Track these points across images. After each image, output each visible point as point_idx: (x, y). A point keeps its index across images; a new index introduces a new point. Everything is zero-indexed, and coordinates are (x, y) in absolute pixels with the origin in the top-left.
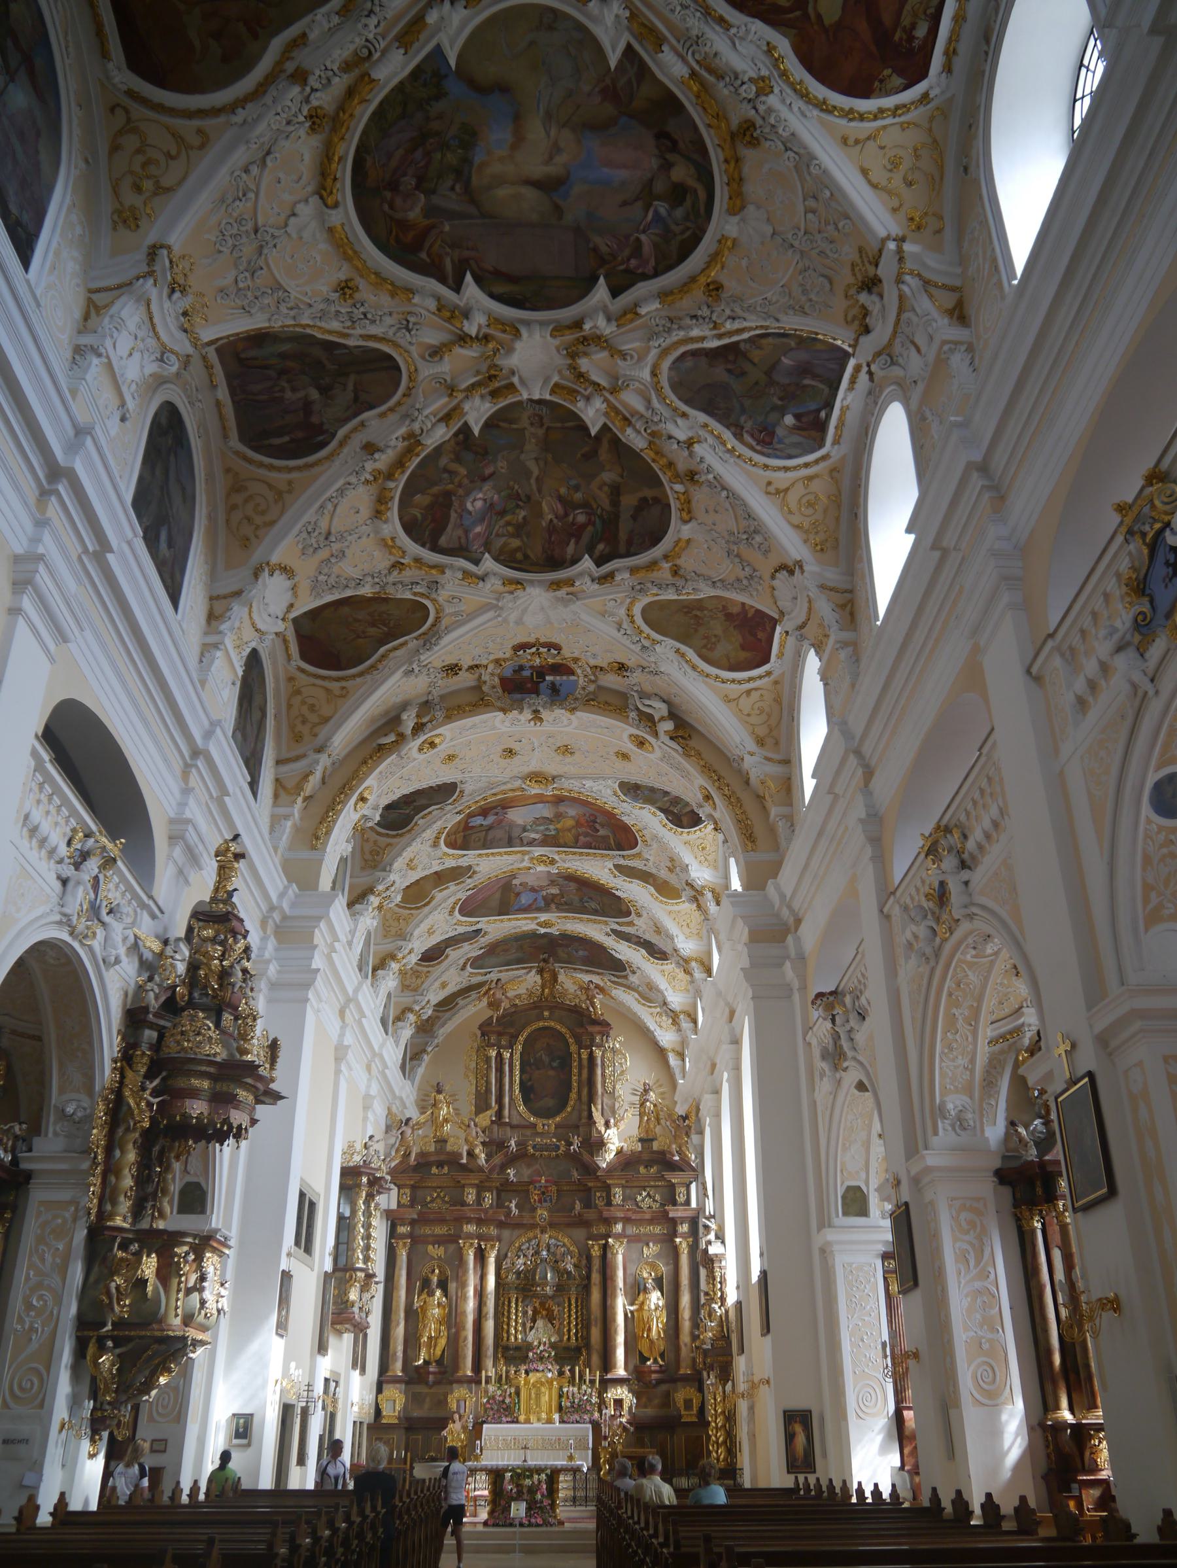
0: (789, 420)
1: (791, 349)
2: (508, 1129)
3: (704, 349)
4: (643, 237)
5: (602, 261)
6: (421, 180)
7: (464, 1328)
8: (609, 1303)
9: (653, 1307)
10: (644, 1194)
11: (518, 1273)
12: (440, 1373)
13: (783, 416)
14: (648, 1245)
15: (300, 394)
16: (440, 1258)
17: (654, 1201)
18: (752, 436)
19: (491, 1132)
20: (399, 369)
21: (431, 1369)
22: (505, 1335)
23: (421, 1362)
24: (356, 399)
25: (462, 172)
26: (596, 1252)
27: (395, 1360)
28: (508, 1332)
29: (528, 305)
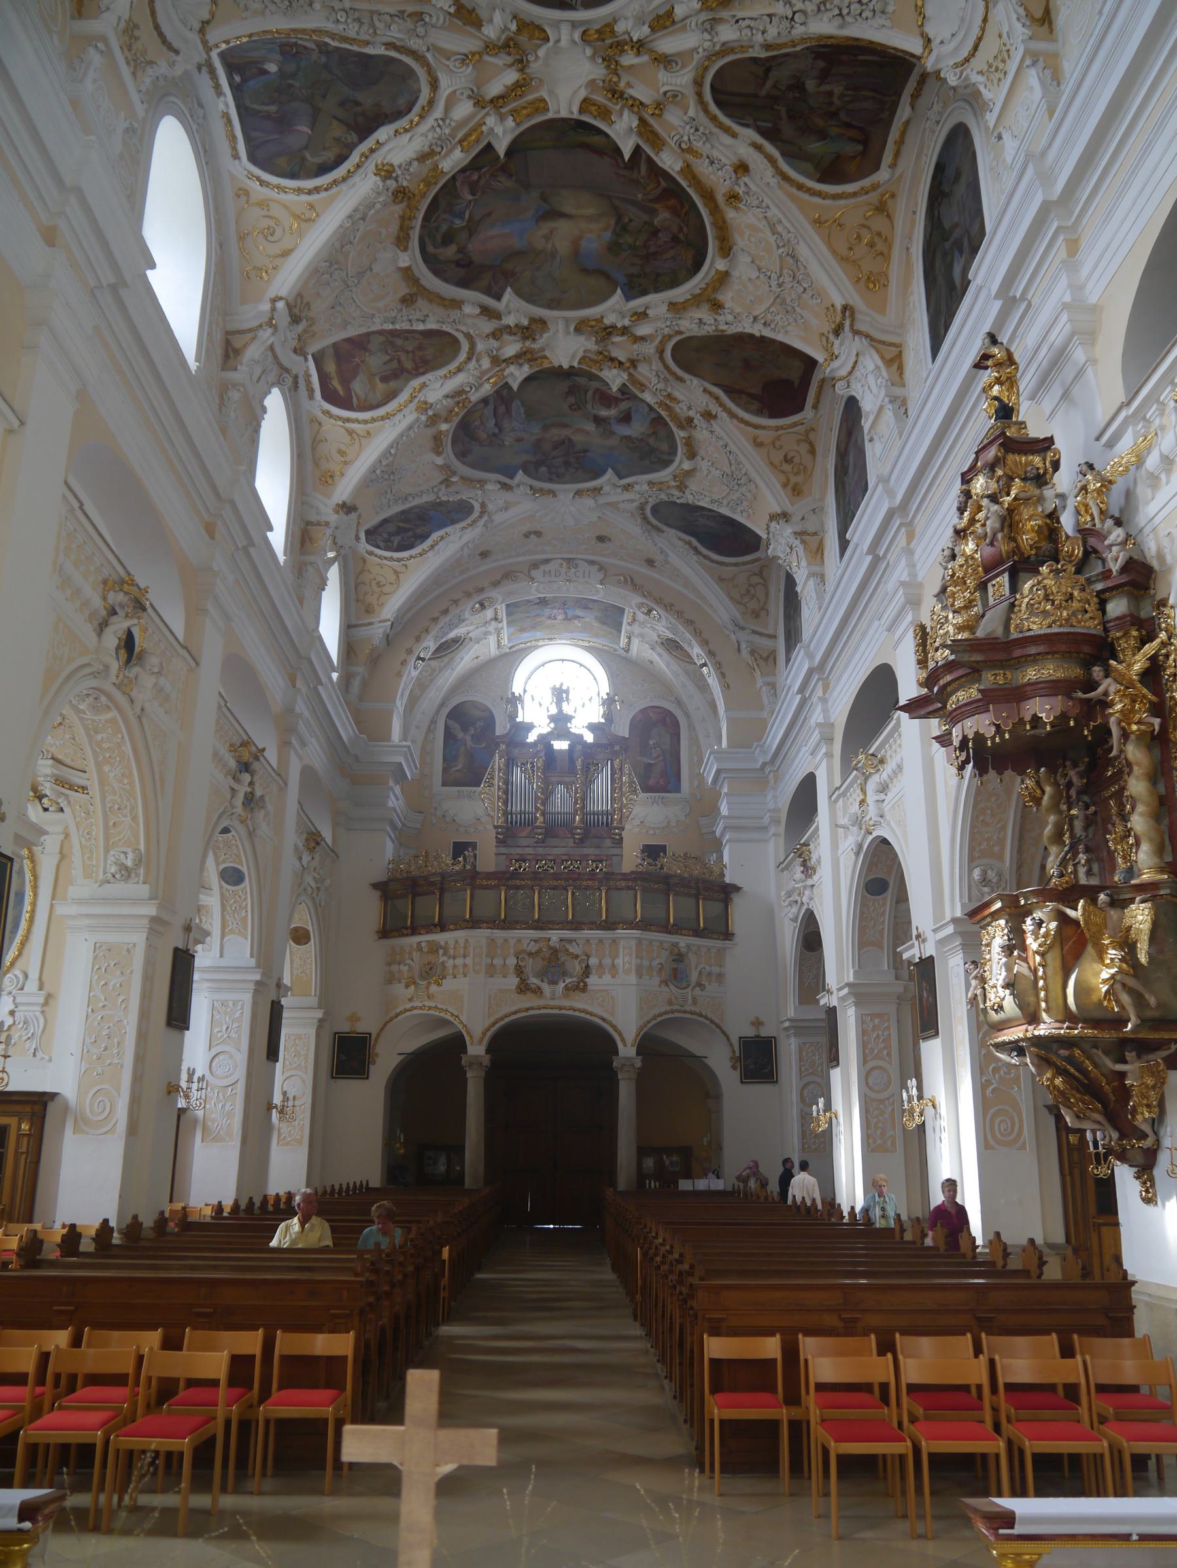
0: (272, 68)
1: (306, 147)
3: (391, 122)
4: (470, 197)
5: (504, 169)
6: (655, 233)
13: (280, 70)
15: (826, 88)
18: (305, 48)
20: (713, 88)
24: (768, 70)
25: (622, 228)
29: (572, 123)
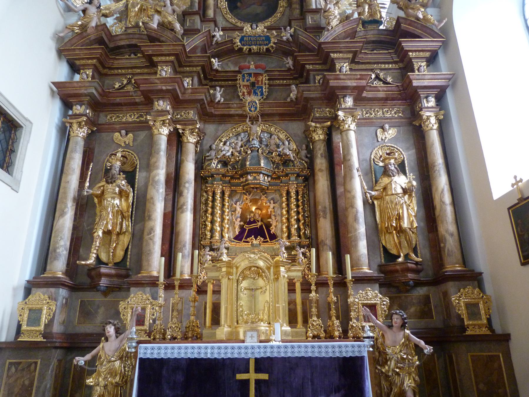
2: (212, 25)
7: (150, 218)
8: (340, 190)
9: (400, 191)
10: (373, 76)
11: (225, 163)
12: (118, 276)
14: (382, 128)
16: (127, 146)
17: (385, 83)
19: (193, 22)
21: (103, 270)
22: (209, 234)
23: (91, 261)
26: (319, 136)
27: (56, 258)
28: (212, 231)
